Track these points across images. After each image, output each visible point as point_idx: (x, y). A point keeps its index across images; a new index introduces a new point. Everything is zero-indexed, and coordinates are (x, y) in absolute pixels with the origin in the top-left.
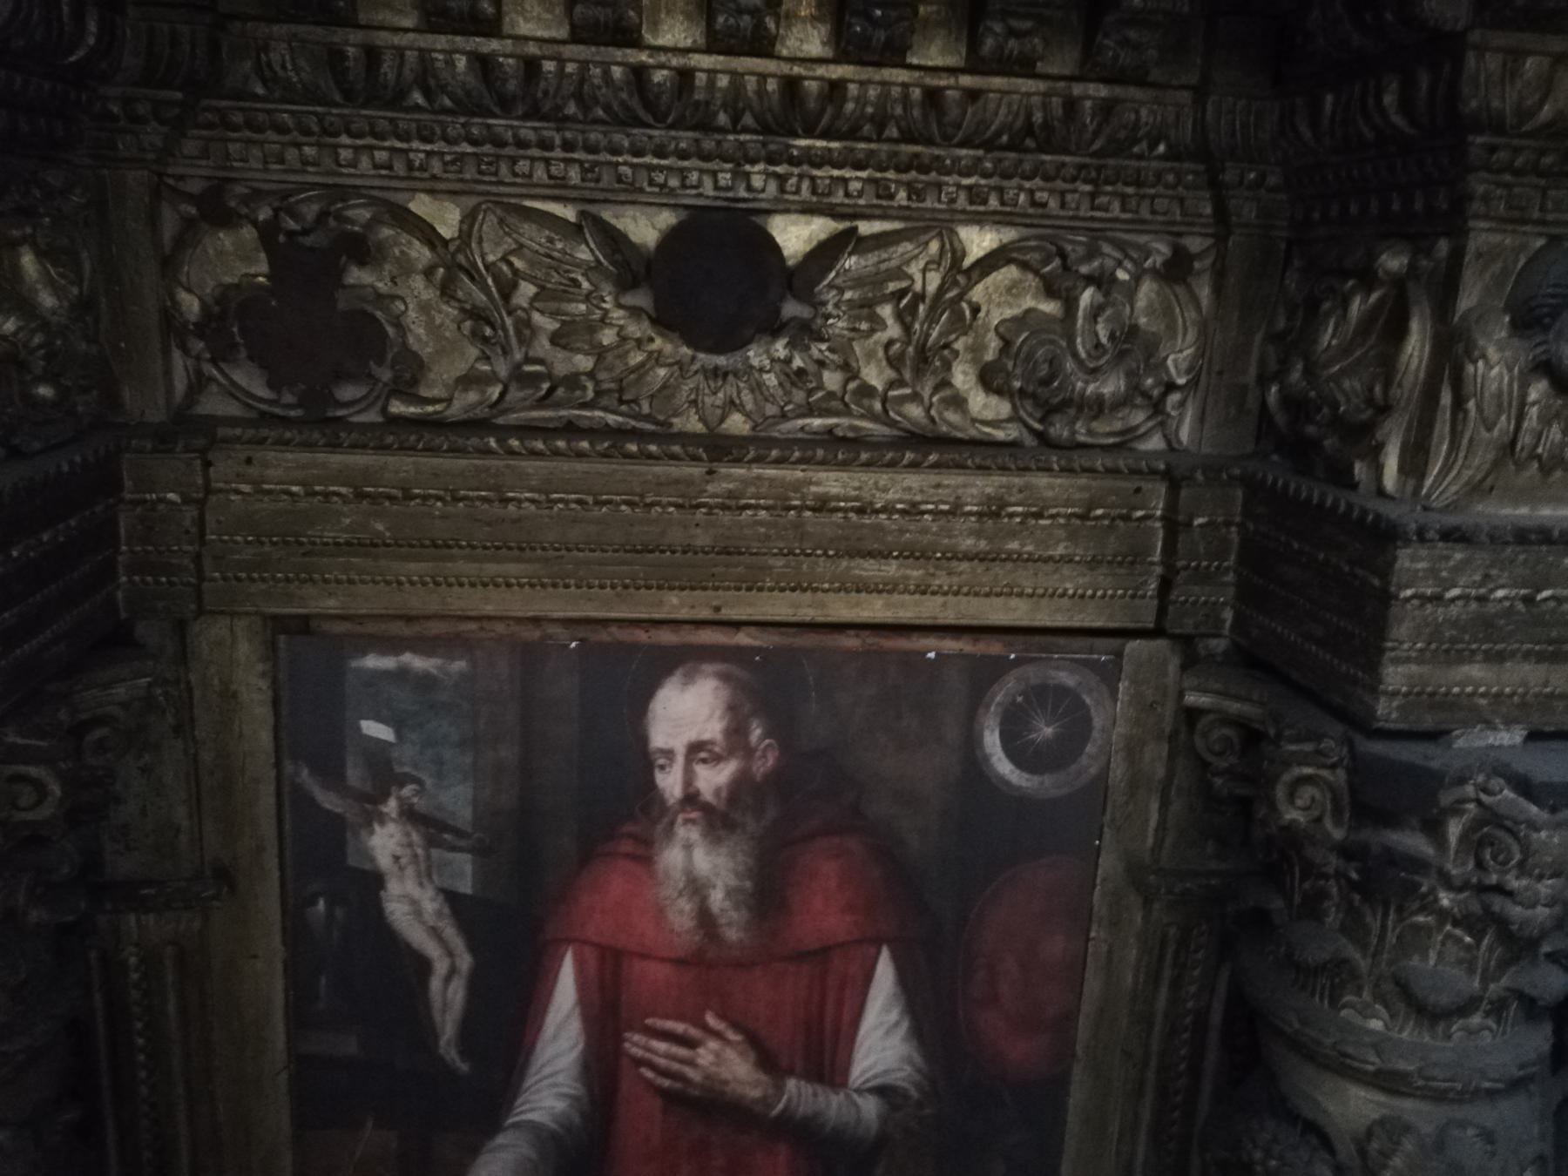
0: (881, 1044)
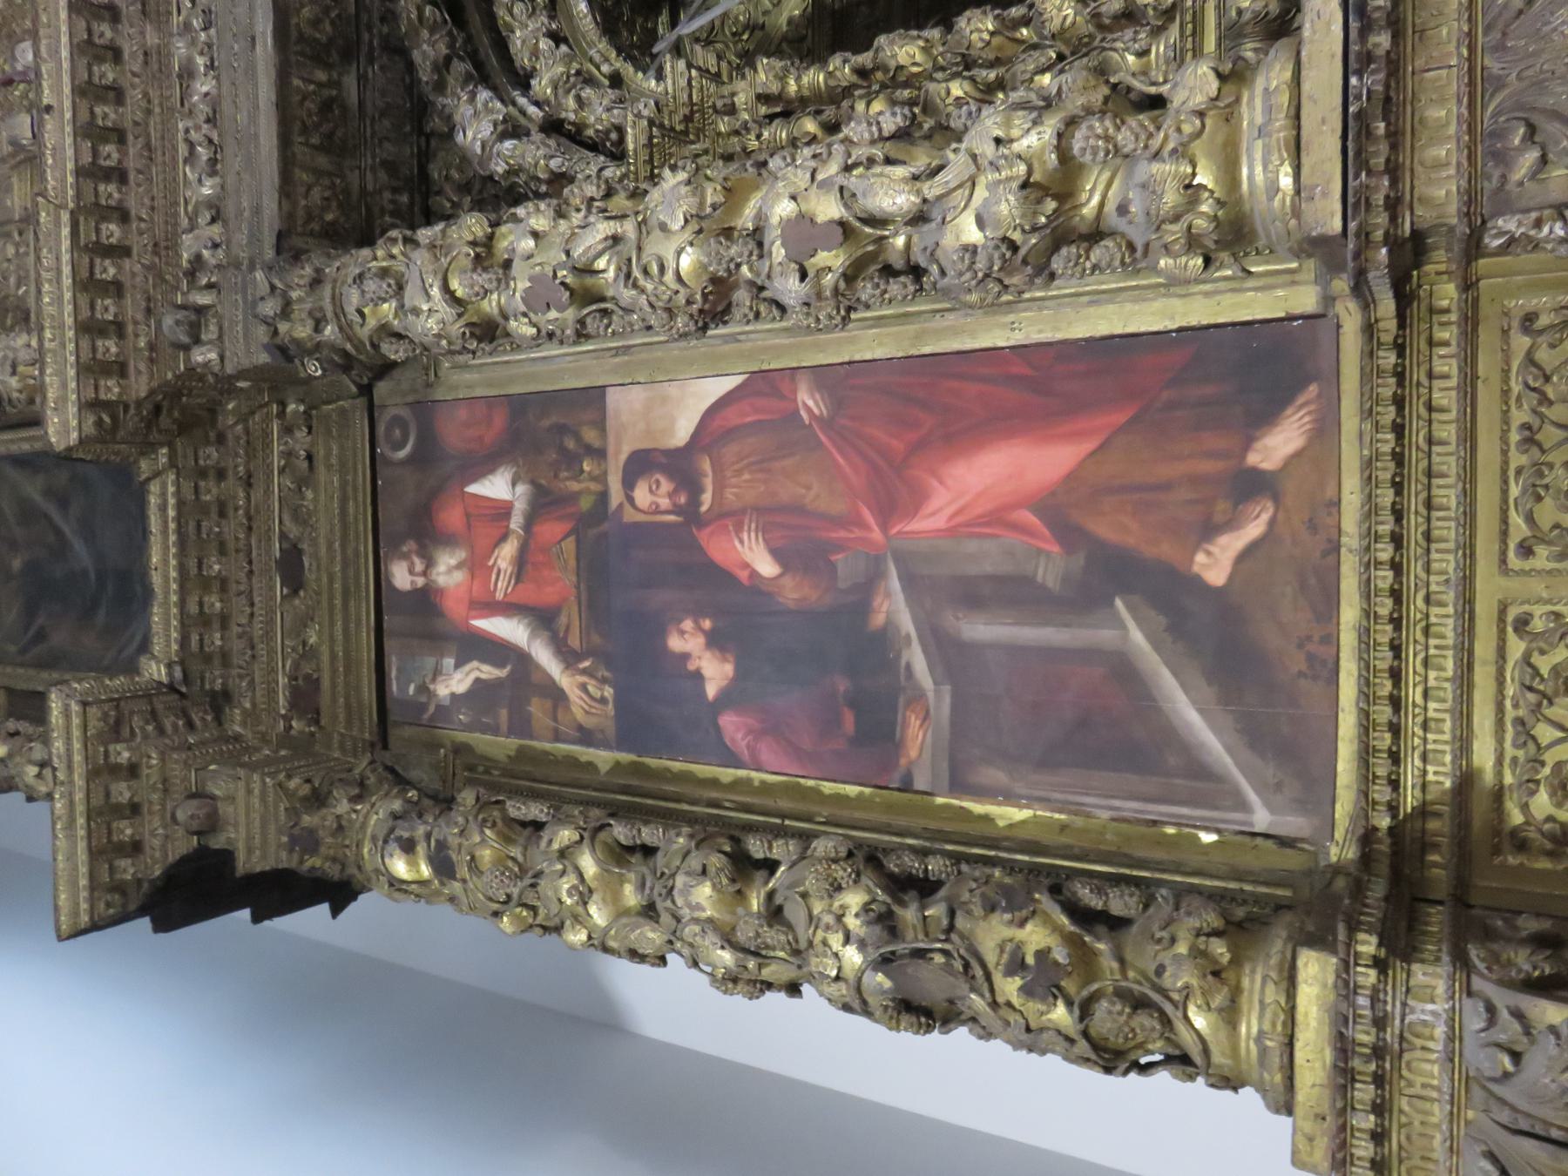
0: (496, 486)
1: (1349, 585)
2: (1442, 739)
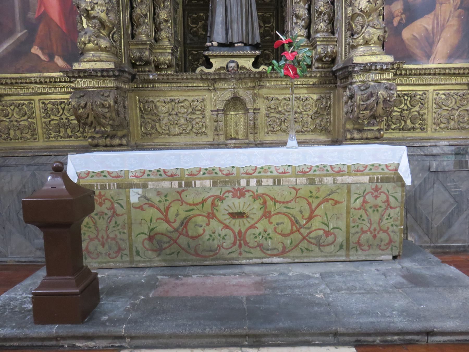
1: (34, 75)
2: (8, 91)
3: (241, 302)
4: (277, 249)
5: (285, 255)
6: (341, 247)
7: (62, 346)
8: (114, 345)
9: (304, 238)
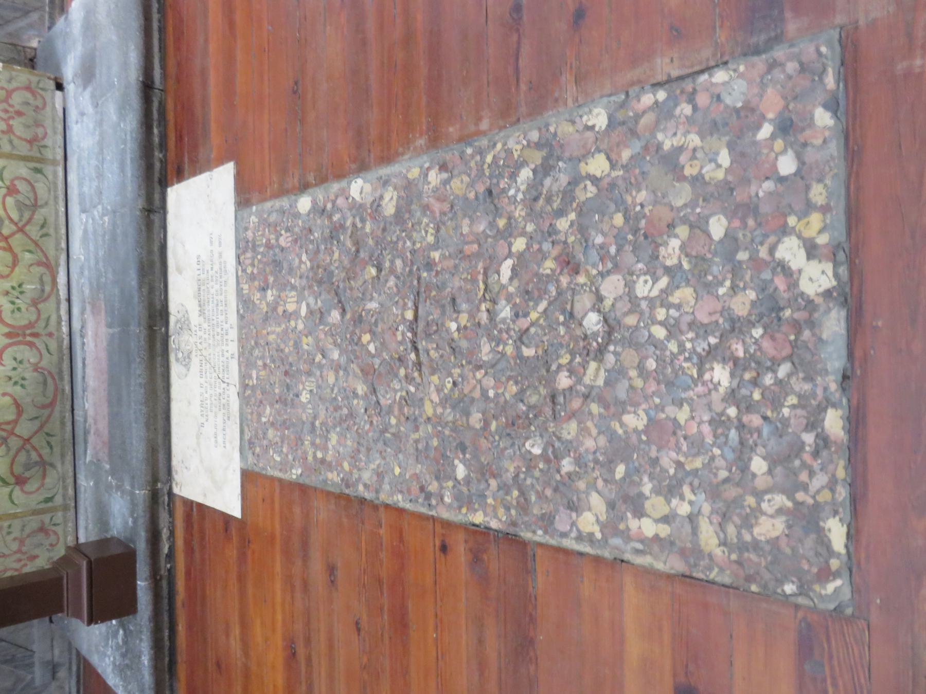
3: (112, 335)
4: (41, 276)
5: (53, 263)
6: (38, 171)
7: (169, 570)
8: (166, 503)
9: (21, 230)
